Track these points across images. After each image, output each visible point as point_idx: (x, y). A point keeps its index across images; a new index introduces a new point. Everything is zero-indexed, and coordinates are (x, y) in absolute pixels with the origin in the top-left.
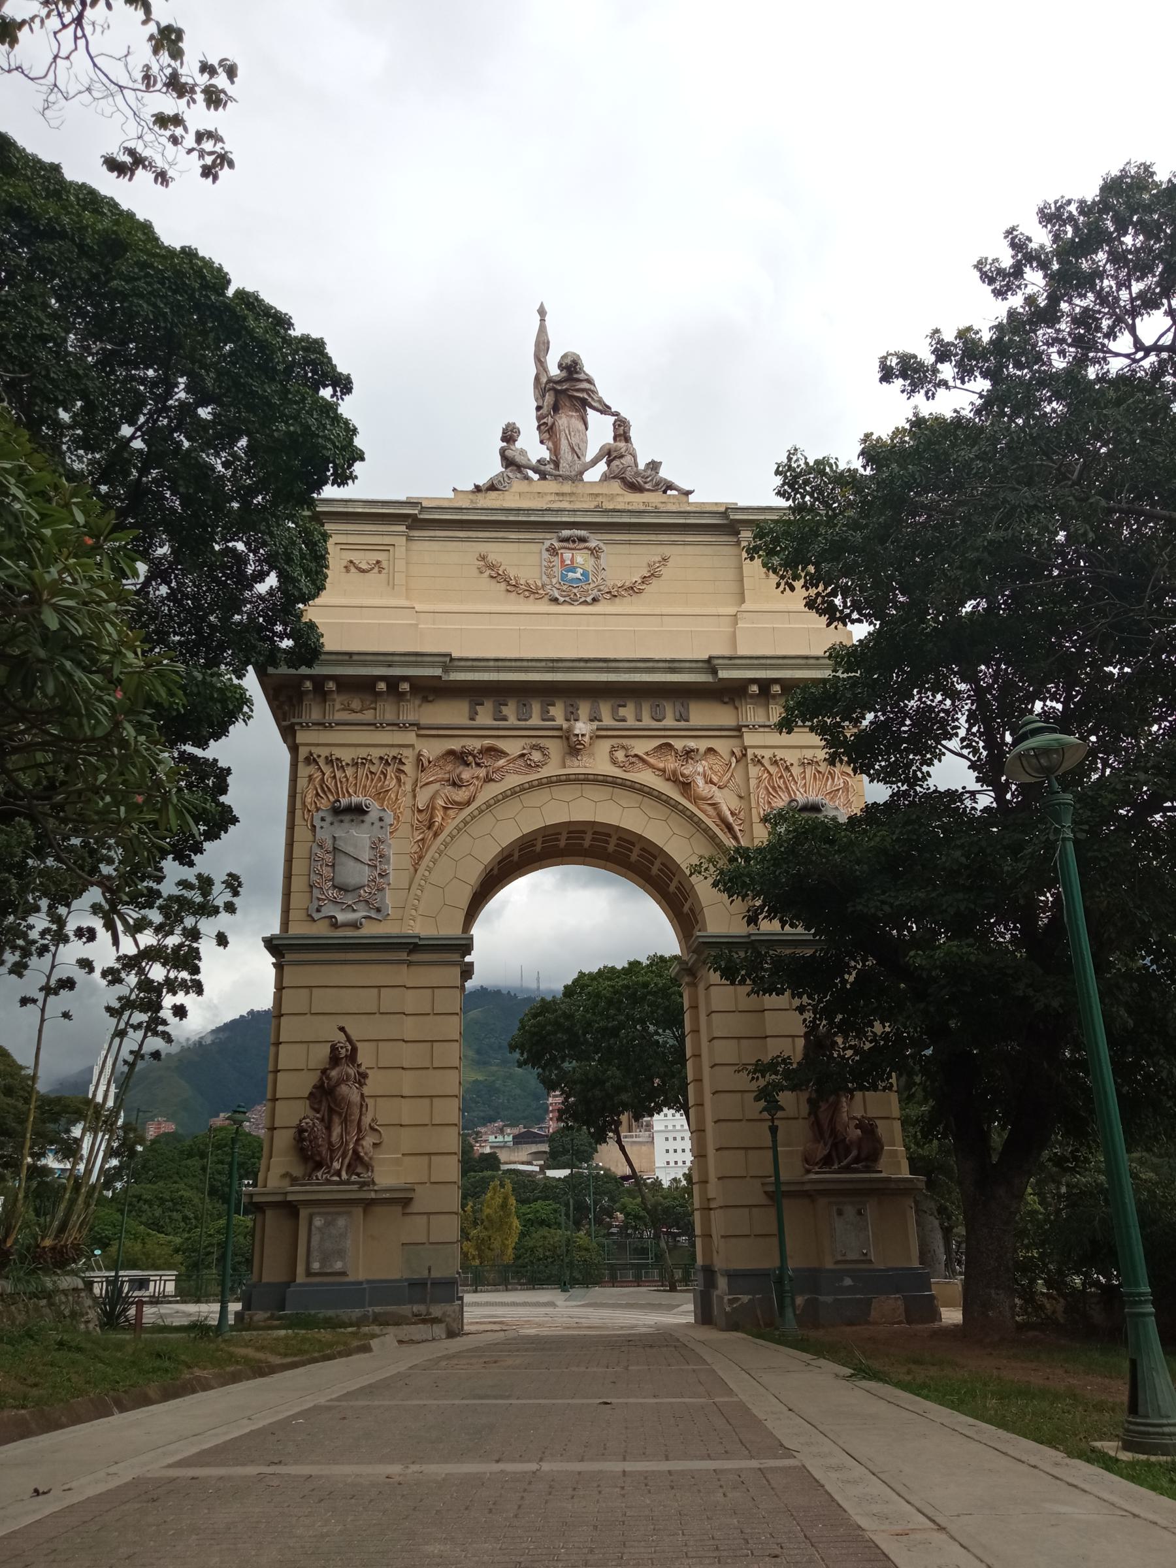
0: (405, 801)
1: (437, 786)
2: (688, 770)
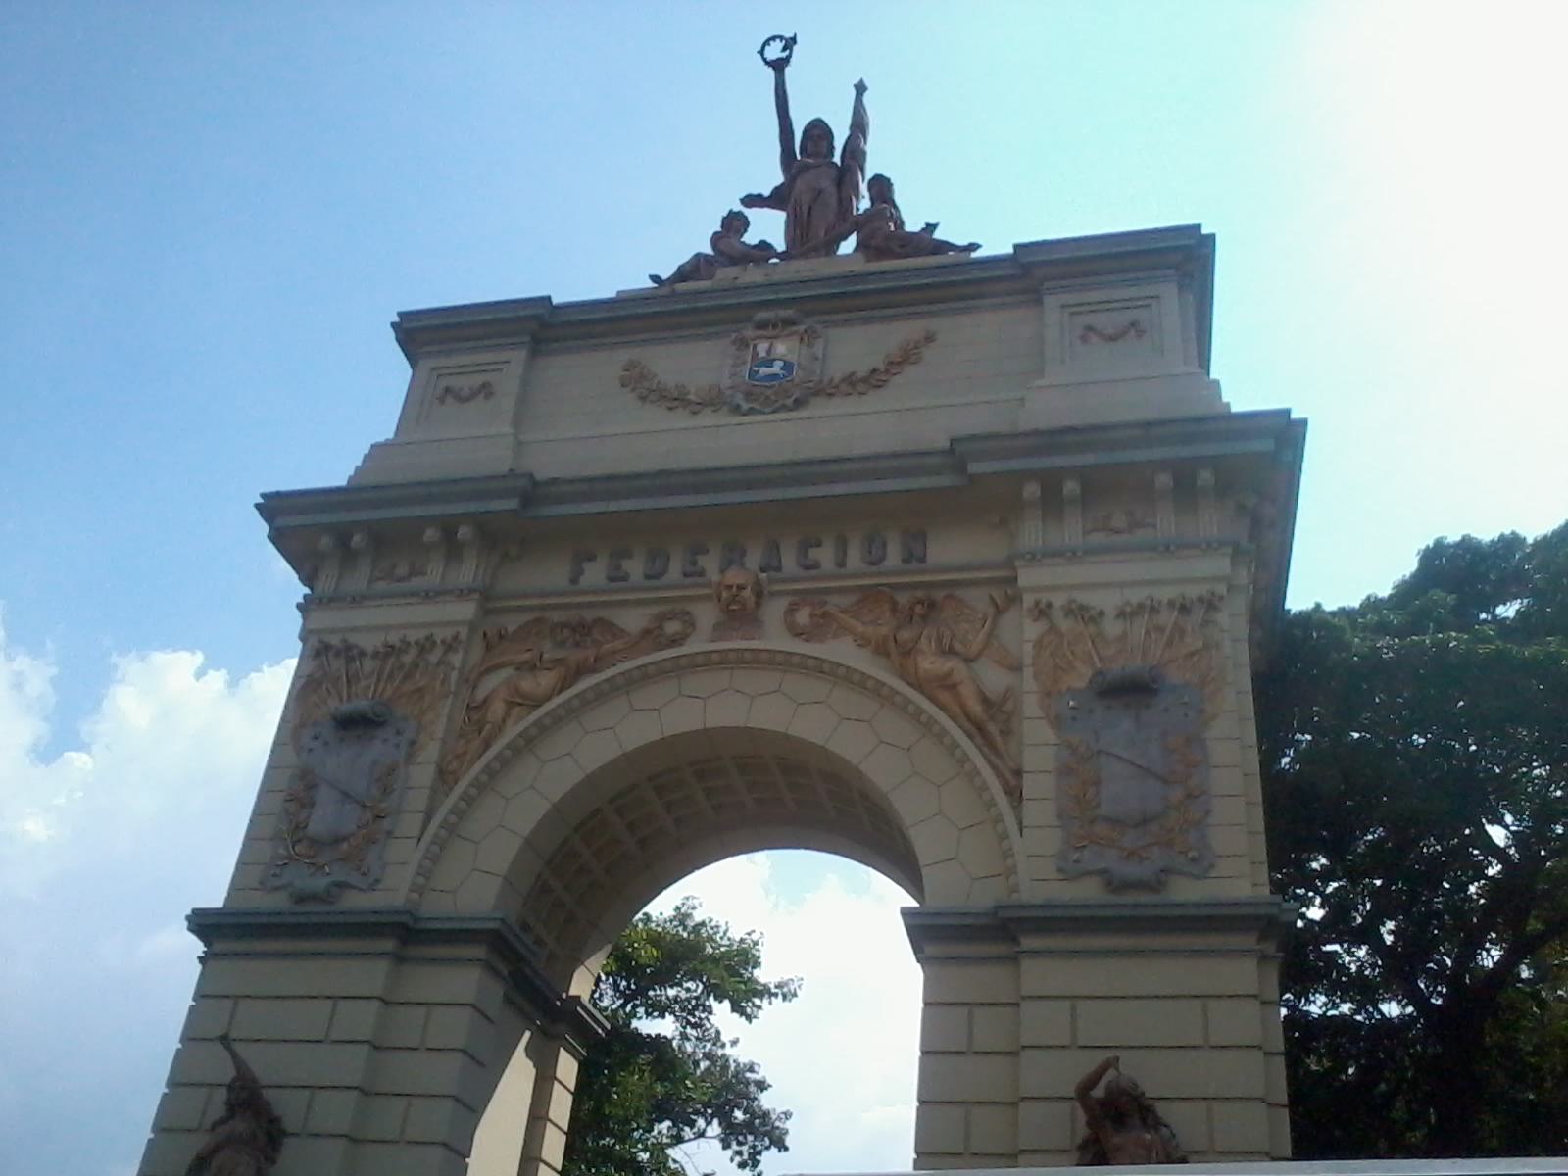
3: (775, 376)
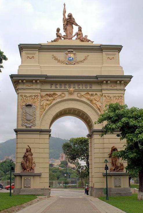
1: (44, 101)
2: (92, 98)
3: (71, 60)
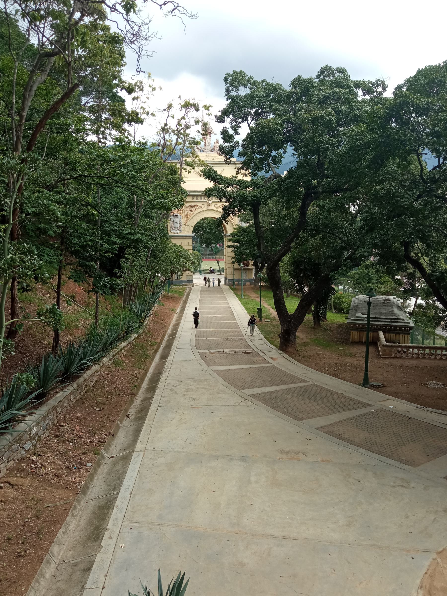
0: (183, 214)
